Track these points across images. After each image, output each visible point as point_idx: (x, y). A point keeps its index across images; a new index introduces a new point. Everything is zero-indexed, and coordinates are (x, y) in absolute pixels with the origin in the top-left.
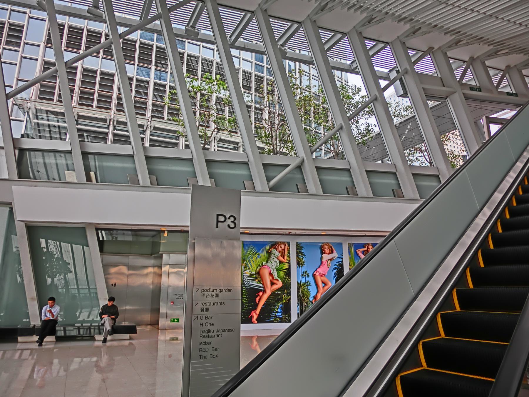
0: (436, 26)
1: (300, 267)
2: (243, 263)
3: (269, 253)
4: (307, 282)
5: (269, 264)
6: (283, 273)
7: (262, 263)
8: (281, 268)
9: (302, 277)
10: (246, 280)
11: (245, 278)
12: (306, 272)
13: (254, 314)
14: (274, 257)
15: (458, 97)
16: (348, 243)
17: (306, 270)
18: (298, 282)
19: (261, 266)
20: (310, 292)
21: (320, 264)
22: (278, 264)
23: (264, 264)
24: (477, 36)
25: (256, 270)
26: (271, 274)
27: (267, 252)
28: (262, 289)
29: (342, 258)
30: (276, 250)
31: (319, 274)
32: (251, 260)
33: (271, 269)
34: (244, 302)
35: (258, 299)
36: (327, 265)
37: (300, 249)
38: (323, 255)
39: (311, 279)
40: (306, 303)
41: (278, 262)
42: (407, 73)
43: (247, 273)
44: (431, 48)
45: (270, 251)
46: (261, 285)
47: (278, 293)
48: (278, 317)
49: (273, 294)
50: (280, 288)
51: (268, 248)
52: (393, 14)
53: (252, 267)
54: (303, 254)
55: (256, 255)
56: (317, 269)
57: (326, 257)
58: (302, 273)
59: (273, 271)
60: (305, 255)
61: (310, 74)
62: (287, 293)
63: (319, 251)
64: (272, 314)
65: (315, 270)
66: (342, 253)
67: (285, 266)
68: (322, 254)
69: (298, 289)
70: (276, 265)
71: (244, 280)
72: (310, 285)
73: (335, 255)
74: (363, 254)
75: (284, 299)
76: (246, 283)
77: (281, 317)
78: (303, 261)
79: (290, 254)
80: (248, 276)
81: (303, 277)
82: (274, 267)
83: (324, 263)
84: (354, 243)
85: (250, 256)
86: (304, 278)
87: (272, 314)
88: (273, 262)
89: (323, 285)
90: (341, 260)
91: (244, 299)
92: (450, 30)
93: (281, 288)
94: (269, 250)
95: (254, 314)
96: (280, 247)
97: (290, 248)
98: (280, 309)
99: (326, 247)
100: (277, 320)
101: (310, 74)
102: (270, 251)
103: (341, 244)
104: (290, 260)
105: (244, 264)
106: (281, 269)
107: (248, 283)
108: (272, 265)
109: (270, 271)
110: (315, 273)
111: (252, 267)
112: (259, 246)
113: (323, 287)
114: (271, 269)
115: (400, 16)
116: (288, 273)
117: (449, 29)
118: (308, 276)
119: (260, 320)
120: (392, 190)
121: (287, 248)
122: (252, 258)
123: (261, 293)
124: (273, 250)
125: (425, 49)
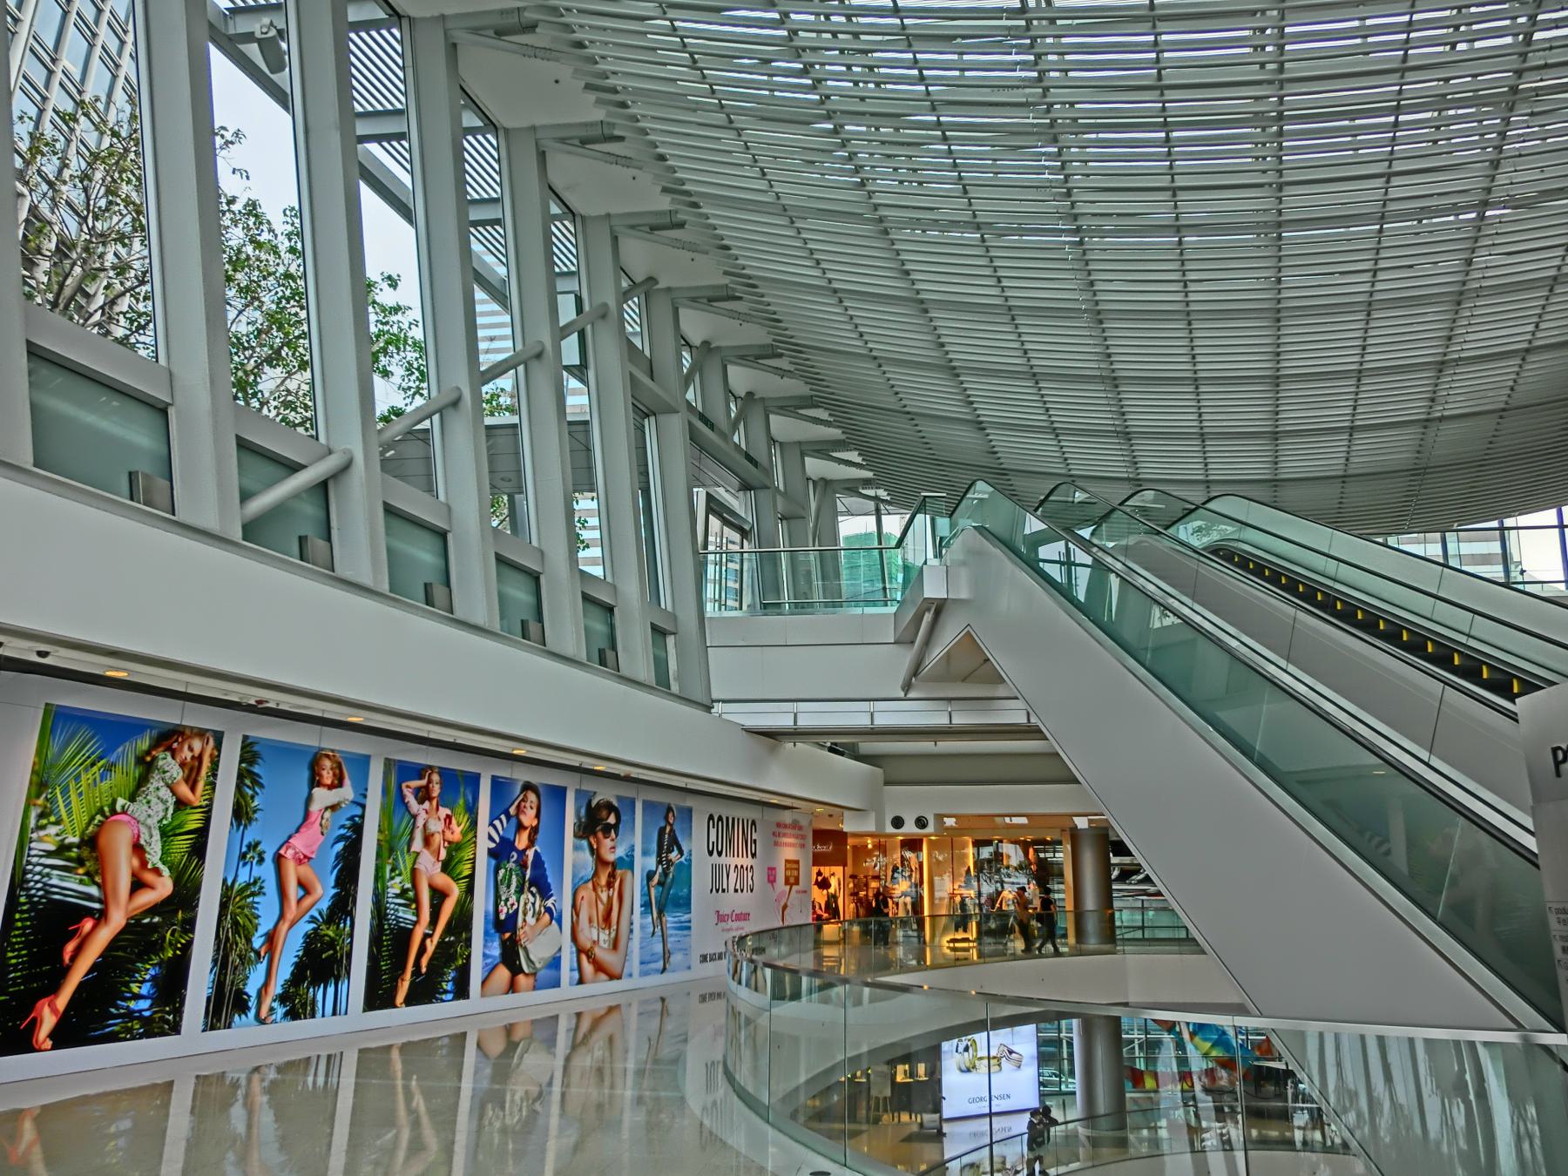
0: (727, 248)
1: (242, 828)
2: (38, 797)
3: (147, 766)
4: (255, 882)
5: (138, 809)
6: (181, 845)
7: (114, 801)
8: (180, 826)
9: (241, 864)
10: (38, 869)
11: (34, 860)
12: (257, 844)
13: (46, 1012)
14: (162, 784)
15: (676, 425)
16: (386, 759)
17: (258, 839)
18: (225, 881)
19: (108, 814)
20: (258, 917)
21: (300, 820)
22: (171, 811)
23: (118, 808)
24: (775, 313)
25: (87, 828)
26: (138, 849)
27: (140, 760)
28: (97, 906)
29: (363, 807)
30: (173, 757)
31: (296, 853)
32: (72, 785)
33: (143, 830)
34: (13, 961)
35: (70, 947)
36: (321, 825)
37: (252, 762)
38: (316, 791)
39: (267, 871)
40: (240, 956)
41: (171, 801)
42: (604, 317)
43: (47, 839)
44: (651, 280)
45: (148, 759)
46: (94, 891)
47: (150, 923)
48: (137, 1018)
49: (133, 928)
50: (162, 902)
51: (144, 744)
52: (673, 170)
53: (70, 813)
54: (256, 781)
55: (95, 769)
56: (290, 837)
57: (322, 797)
58: (244, 849)
59: (147, 837)
60: (262, 786)
61: (44, 99)
62: (185, 921)
63: (306, 774)
64: (118, 1008)
65: (285, 838)
66: (366, 790)
67: (193, 821)
68: (312, 787)
69: (224, 906)
70: (161, 814)
71: (30, 867)
72: (260, 892)
73: (347, 792)
74: (416, 798)
75: (171, 944)
76: (37, 882)
77: (147, 1014)
78: (253, 805)
79: (215, 776)
80: (49, 854)
81: (245, 864)
82: (153, 822)
83: (312, 819)
84: (400, 761)
85: (70, 769)
86: (248, 867)
87: (118, 1008)
88: (154, 801)
89: (301, 893)
90: (358, 811)
91: (13, 951)
92: (744, 271)
93: (167, 902)
94: (148, 753)
95: (46, 1012)
96: (186, 747)
97: (219, 756)
98: (149, 984)
99: (327, 763)
100: (130, 1030)
101: (44, 99)
102: (148, 759)
103: (366, 759)
104: (211, 800)
105: (40, 801)
106: (178, 831)
107: (45, 880)
108: (150, 812)
109: (139, 836)
110: (282, 852)
111: (70, 813)
112: (114, 730)
113: (299, 901)
114: (140, 826)
115: (682, 182)
116: (198, 849)
117: (744, 269)
118: (261, 860)
119: (68, 1035)
120: (522, 621)
121: (211, 755)
122: (78, 778)
123: (88, 925)
124: (162, 755)
125: (639, 279)
